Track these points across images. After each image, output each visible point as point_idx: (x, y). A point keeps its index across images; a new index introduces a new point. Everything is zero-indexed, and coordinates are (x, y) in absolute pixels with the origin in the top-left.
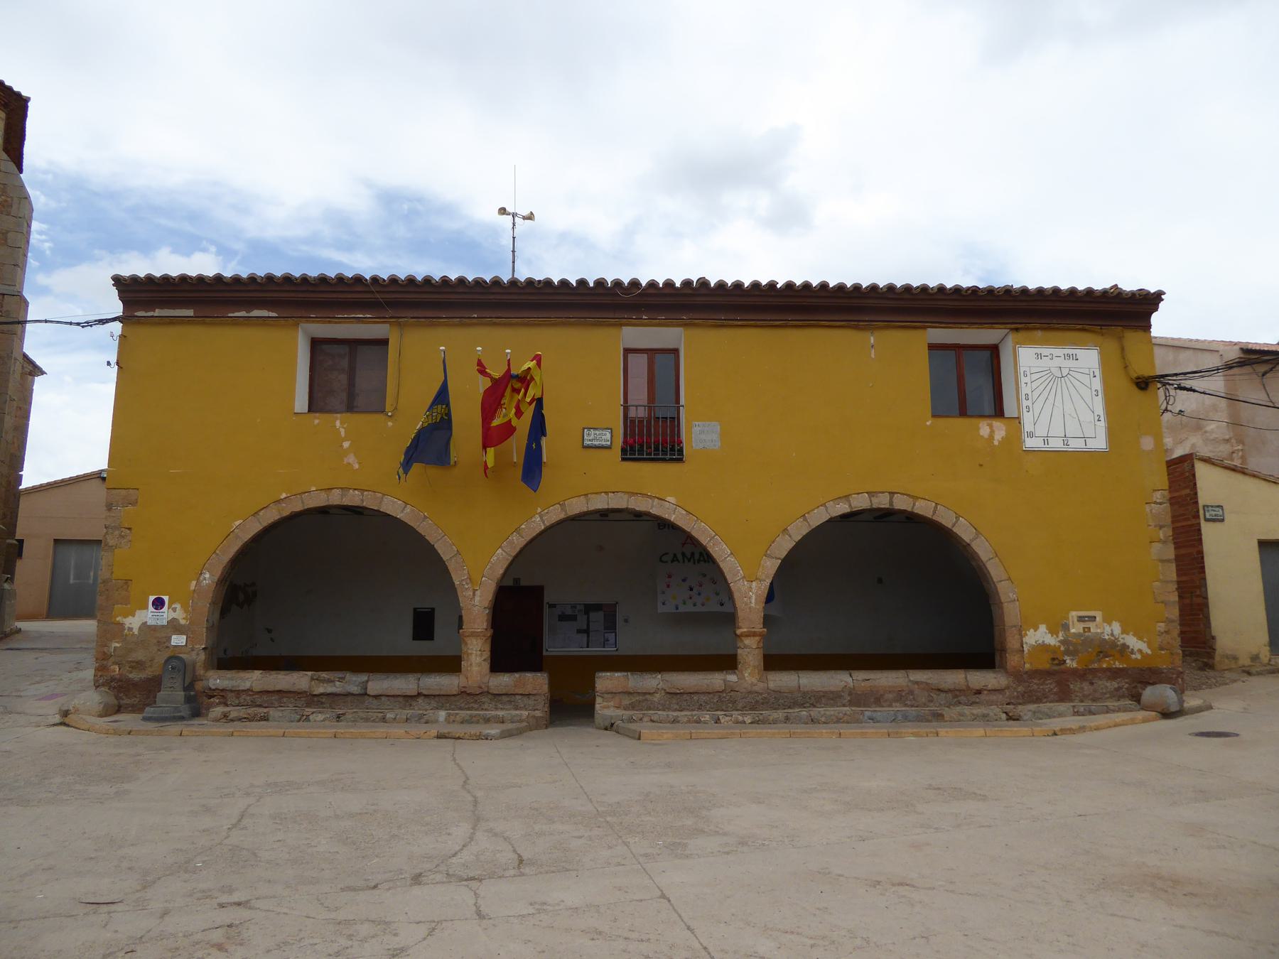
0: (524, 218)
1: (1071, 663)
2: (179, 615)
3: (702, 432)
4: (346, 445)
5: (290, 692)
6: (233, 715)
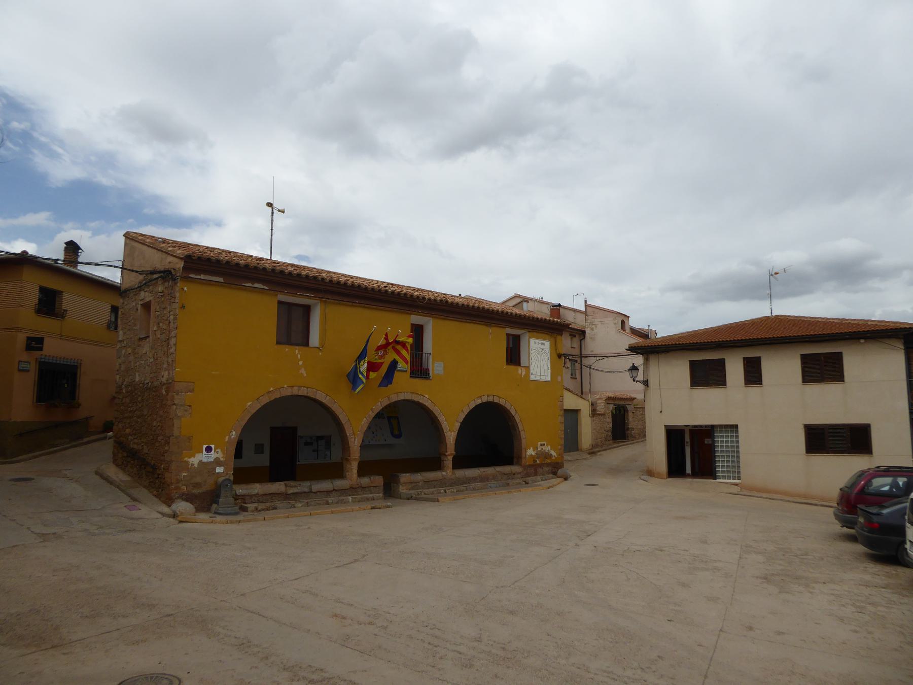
0: (279, 211)
1: (538, 462)
4: (301, 363)
6: (260, 508)
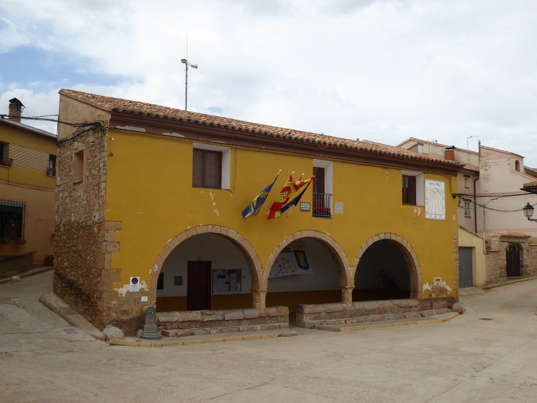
0: (193, 66)
1: (434, 296)
2: (145, 286)
3: (338, 206)
4: (214, 204)
5: (194, 321)
6: (179, 333)
